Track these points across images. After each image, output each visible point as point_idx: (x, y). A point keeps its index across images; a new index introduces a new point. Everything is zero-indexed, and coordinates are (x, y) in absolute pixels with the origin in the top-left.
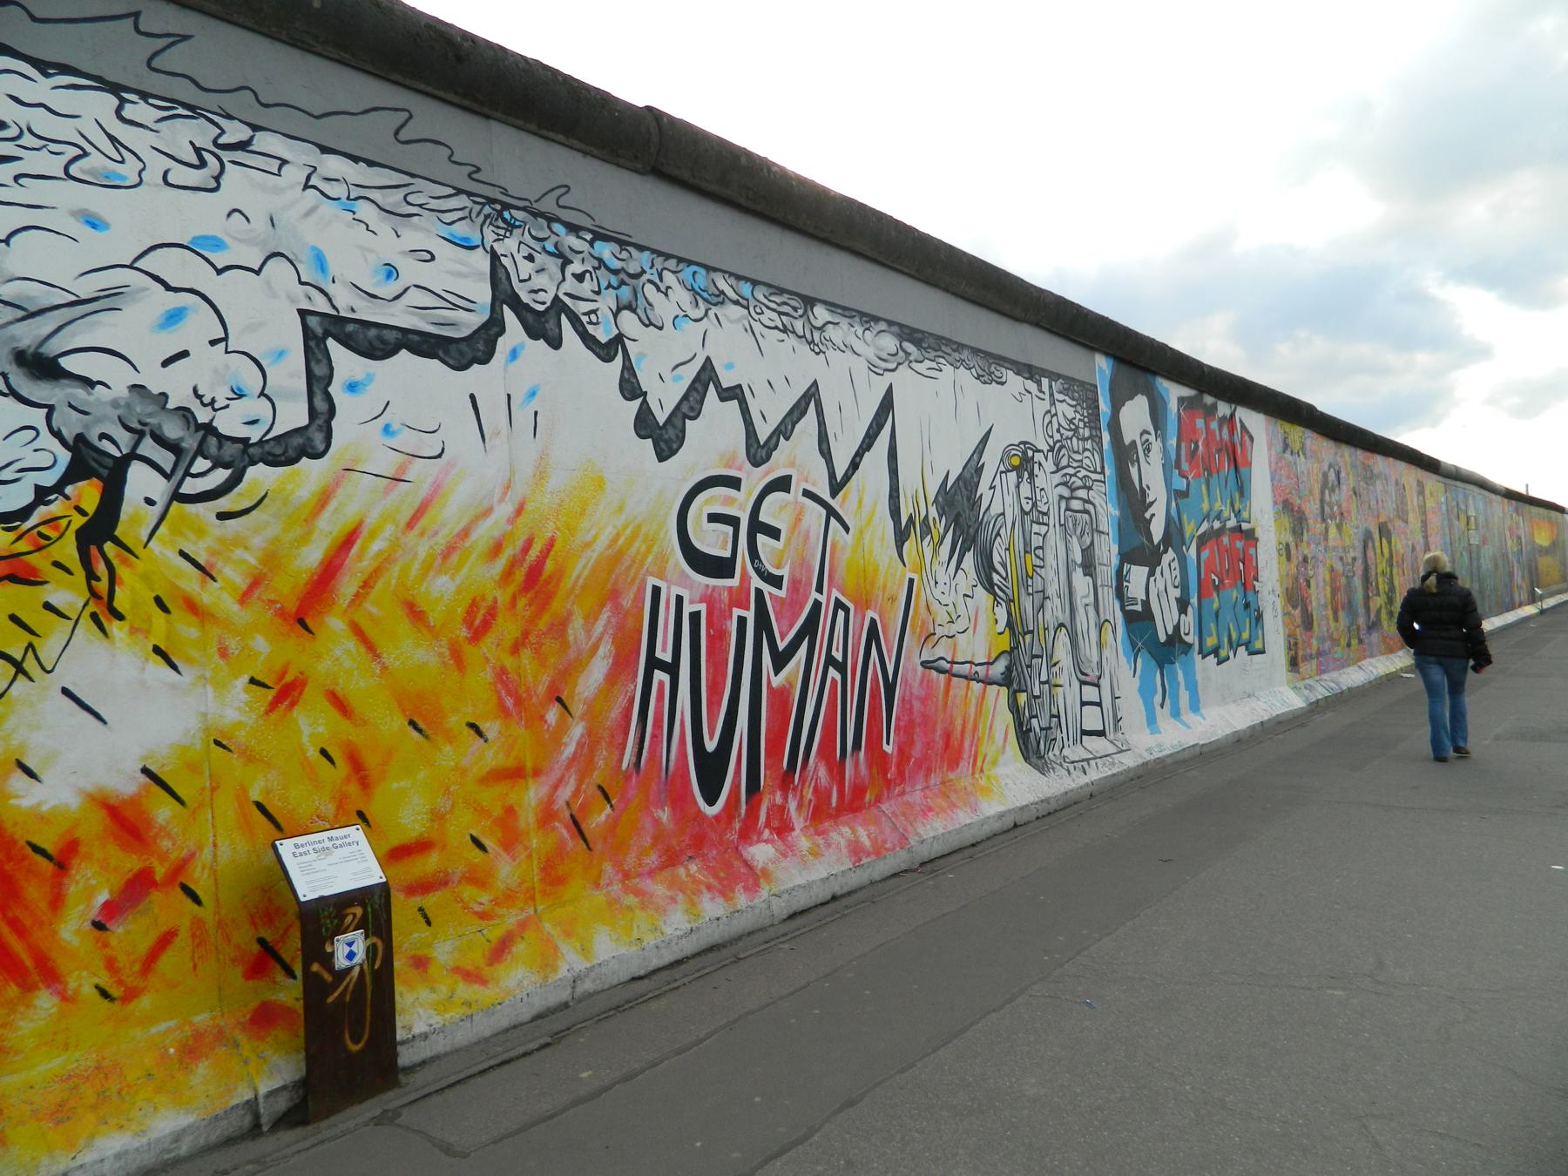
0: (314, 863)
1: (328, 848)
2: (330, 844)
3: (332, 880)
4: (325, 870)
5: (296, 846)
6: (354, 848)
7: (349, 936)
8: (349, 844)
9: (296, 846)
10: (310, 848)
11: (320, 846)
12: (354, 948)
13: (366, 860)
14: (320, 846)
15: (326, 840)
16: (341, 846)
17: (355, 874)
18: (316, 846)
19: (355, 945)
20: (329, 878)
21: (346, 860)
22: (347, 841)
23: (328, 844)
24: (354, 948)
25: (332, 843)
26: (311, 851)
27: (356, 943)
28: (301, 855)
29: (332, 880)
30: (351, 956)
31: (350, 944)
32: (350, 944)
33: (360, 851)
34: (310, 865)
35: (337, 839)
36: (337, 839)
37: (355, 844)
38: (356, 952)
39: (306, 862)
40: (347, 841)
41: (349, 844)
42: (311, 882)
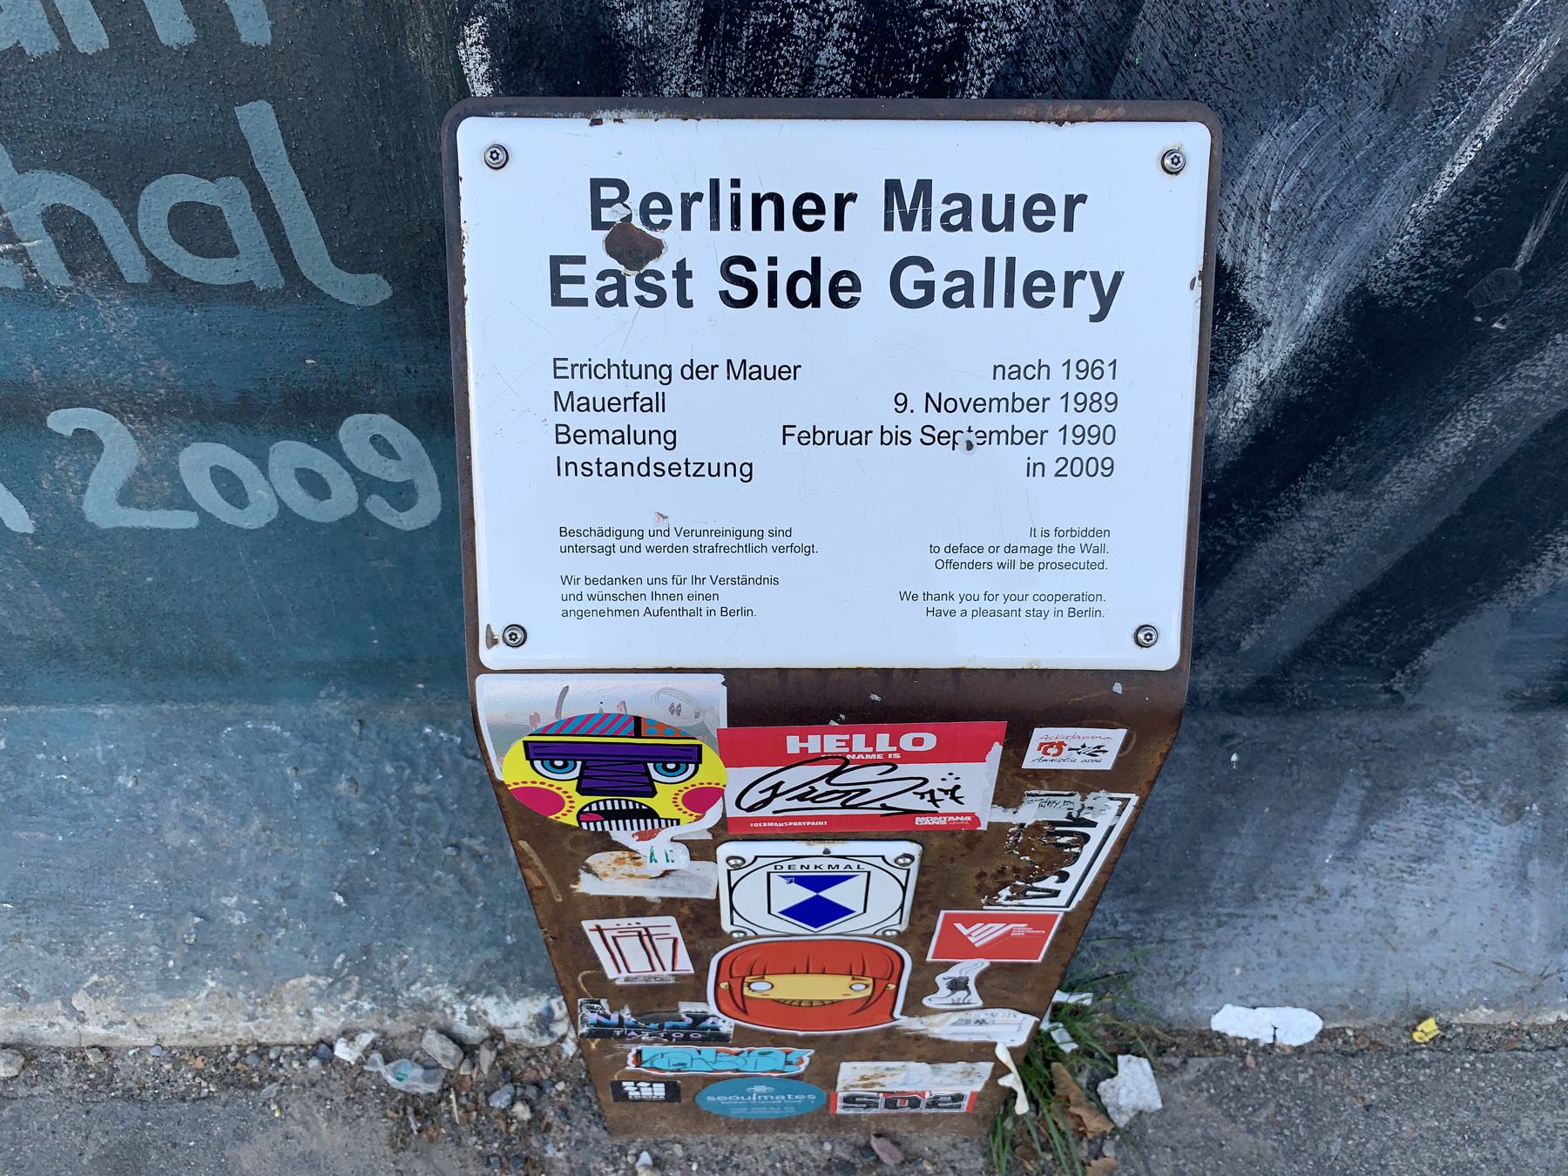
0: (679, 391)
1: (845, 289)
4: (747, 473)
8: (1037, 290)
13: (1107, 468)
15: (868, 211)
16: (961, 292)
17: (955, 556)
18: (746, 242)
20: (746, 540)
33: (1090, 369)
34: (655, 404)
35: (961, 212)
36: (961, 212)
39: (624, 370)
41: (1037, 290)
42: (610, 539)
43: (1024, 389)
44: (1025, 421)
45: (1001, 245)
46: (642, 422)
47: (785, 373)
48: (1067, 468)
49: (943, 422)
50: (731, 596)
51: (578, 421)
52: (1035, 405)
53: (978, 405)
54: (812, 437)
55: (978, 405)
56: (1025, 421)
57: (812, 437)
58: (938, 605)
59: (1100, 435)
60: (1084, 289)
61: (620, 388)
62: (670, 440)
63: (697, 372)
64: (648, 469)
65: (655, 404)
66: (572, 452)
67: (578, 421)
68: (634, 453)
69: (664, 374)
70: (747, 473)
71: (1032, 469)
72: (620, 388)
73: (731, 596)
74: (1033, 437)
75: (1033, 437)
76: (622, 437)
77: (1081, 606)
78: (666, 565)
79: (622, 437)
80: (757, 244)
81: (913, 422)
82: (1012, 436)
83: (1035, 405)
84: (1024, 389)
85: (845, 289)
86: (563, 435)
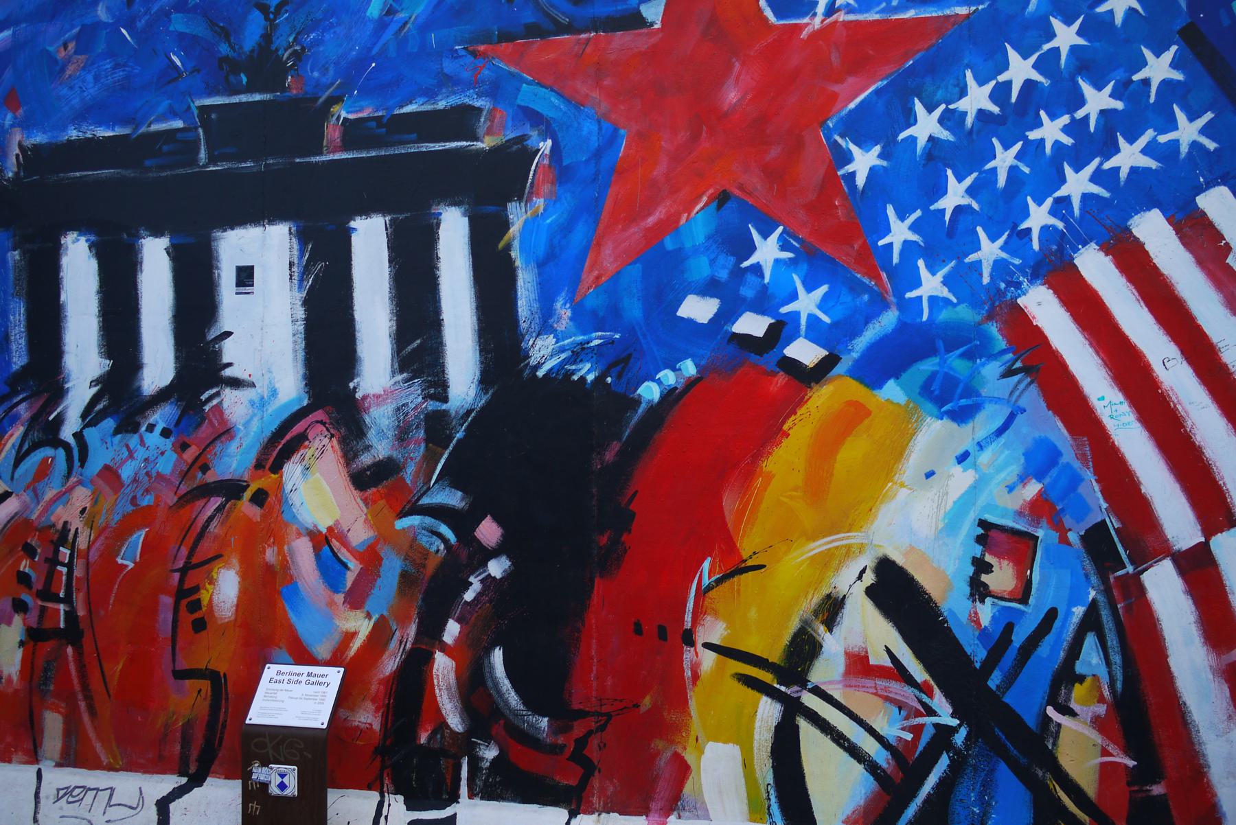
1: (300, 683)
2: (304, 678)
3: (280, 712)
4: (283, 701)
6: (323, 688)
7: (283, 768)
9: (279, 673)
10: (286, 678)
11: (296, 678)
13: (323, 703)
14: (296, 678)
17: (303, 713)
18: (290, 677)
19: (287, 777)
20: (280, 709)
21: (307, 697)
22: (321, 680)
24: (286, 780)
25: (309, 678)
26: (286, 681)
27: (288, 776)
29: (280, 712)
31: (282, 776)
32: (282, 776)
33: (324, 692)
34: (275, 694)
37: (326, 684)
38: (287, 784)
39: (273, 690)
40: (321, 680)
42: (265, 708)
43: (317, 694)
44: (316, 698)
45: (318, 679)
46: (272, 695)
47: (291, 691)
48: (319, 703)
49: (307, 697)
50: (276, 716)
51: (267, 695)
52: (317, 696)
53: (311, 696)
54: (292, 698)
55: (311, 696)
56: (316, 698)
57: (292, 698)
58: (300, 718)
59: (323, 700)
60: (326, 684)
61: (272, 692)
62: (276, 697)
63: (282, 690)
64: (273, 700)
65: (275, 694)
66: (265, 698)
67: (267, 695)
68: (271, 699)
69: (277, 690)
70: (283, 701)
71: (315, 703)
72: (272, 692)
73: (276, 716)
74: (316, 700)
75: (316, 700)
76: (271, 697)
77: (316, 719)
78: (269, 711)
79: (271, 697)
80: (292, 677)
81: (303, 697)
82: (314, 699)
83: (317, 696)
84: (317, 694)
85: (300, 683)
86: (265, 696)
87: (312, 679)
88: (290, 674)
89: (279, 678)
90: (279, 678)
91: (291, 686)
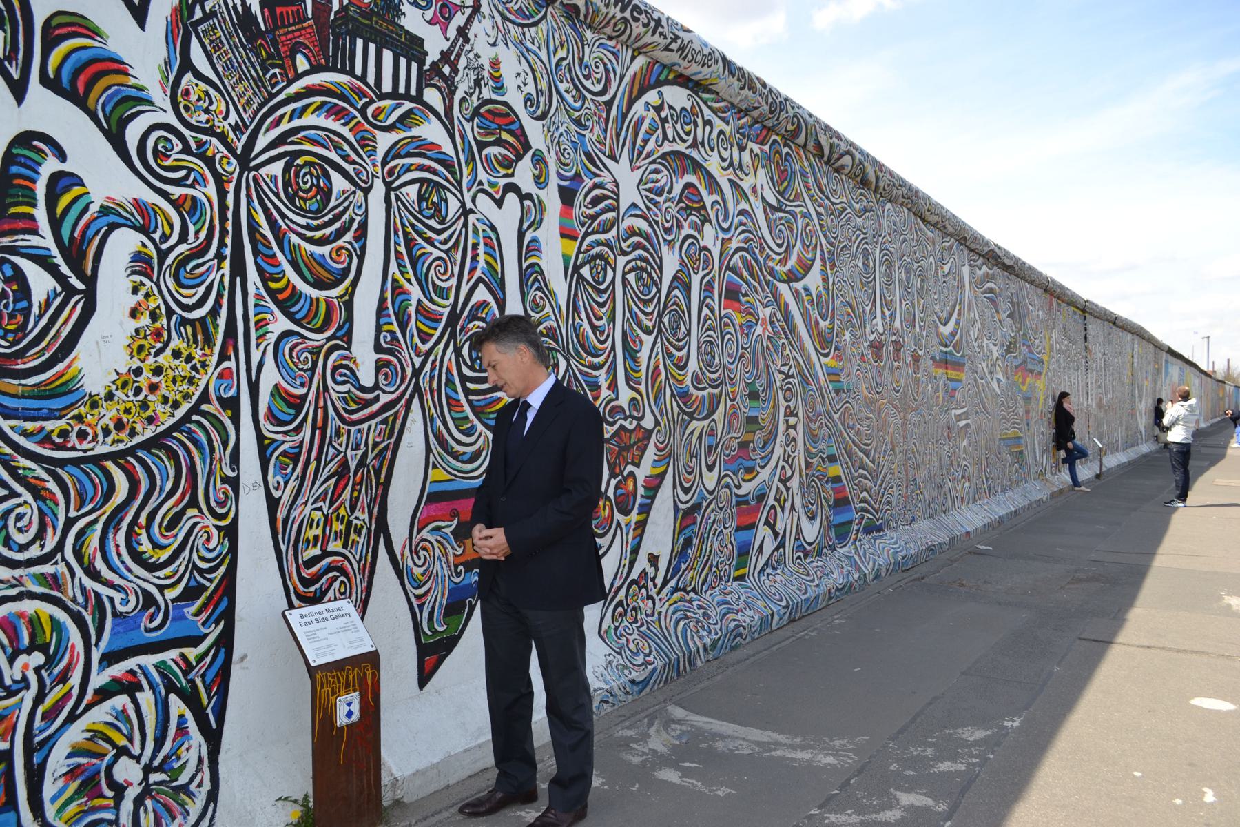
1: (326, 619)
2: (326, 615)
5: (301, 616)
6: (346, 619)
7: (349, 697)
9: (301, 616)
10: (313, 618)
11: (320, 617)
12: (352, 708)
14: (320, 617)
18: (317, 617)
23: (326, 615)
24: (352, 708)
28: (306, 624)
30: (350, 714)
31: (349, 704)
32: (349, 704)
40: (341, 612)
42: (317, 649)
77: (364, 645)
85: (326, 619)
87: (335, 614)
88: (311, 614)
89: (306, 620)
90: (306, 620)
91: (322, 624)
